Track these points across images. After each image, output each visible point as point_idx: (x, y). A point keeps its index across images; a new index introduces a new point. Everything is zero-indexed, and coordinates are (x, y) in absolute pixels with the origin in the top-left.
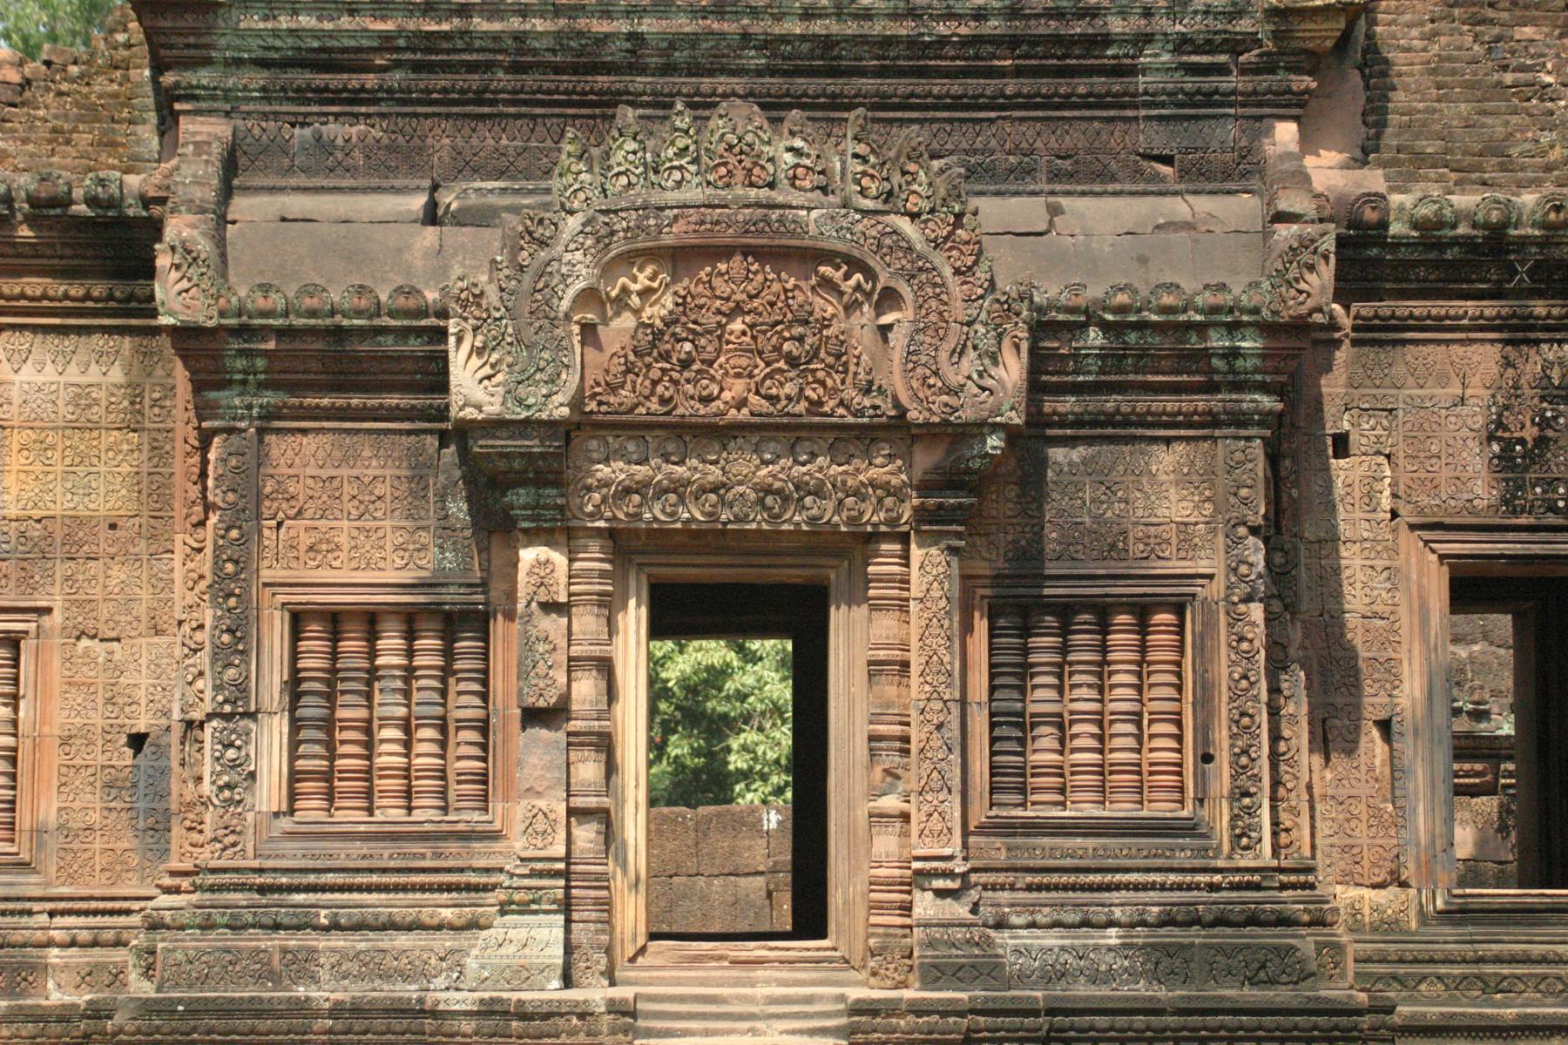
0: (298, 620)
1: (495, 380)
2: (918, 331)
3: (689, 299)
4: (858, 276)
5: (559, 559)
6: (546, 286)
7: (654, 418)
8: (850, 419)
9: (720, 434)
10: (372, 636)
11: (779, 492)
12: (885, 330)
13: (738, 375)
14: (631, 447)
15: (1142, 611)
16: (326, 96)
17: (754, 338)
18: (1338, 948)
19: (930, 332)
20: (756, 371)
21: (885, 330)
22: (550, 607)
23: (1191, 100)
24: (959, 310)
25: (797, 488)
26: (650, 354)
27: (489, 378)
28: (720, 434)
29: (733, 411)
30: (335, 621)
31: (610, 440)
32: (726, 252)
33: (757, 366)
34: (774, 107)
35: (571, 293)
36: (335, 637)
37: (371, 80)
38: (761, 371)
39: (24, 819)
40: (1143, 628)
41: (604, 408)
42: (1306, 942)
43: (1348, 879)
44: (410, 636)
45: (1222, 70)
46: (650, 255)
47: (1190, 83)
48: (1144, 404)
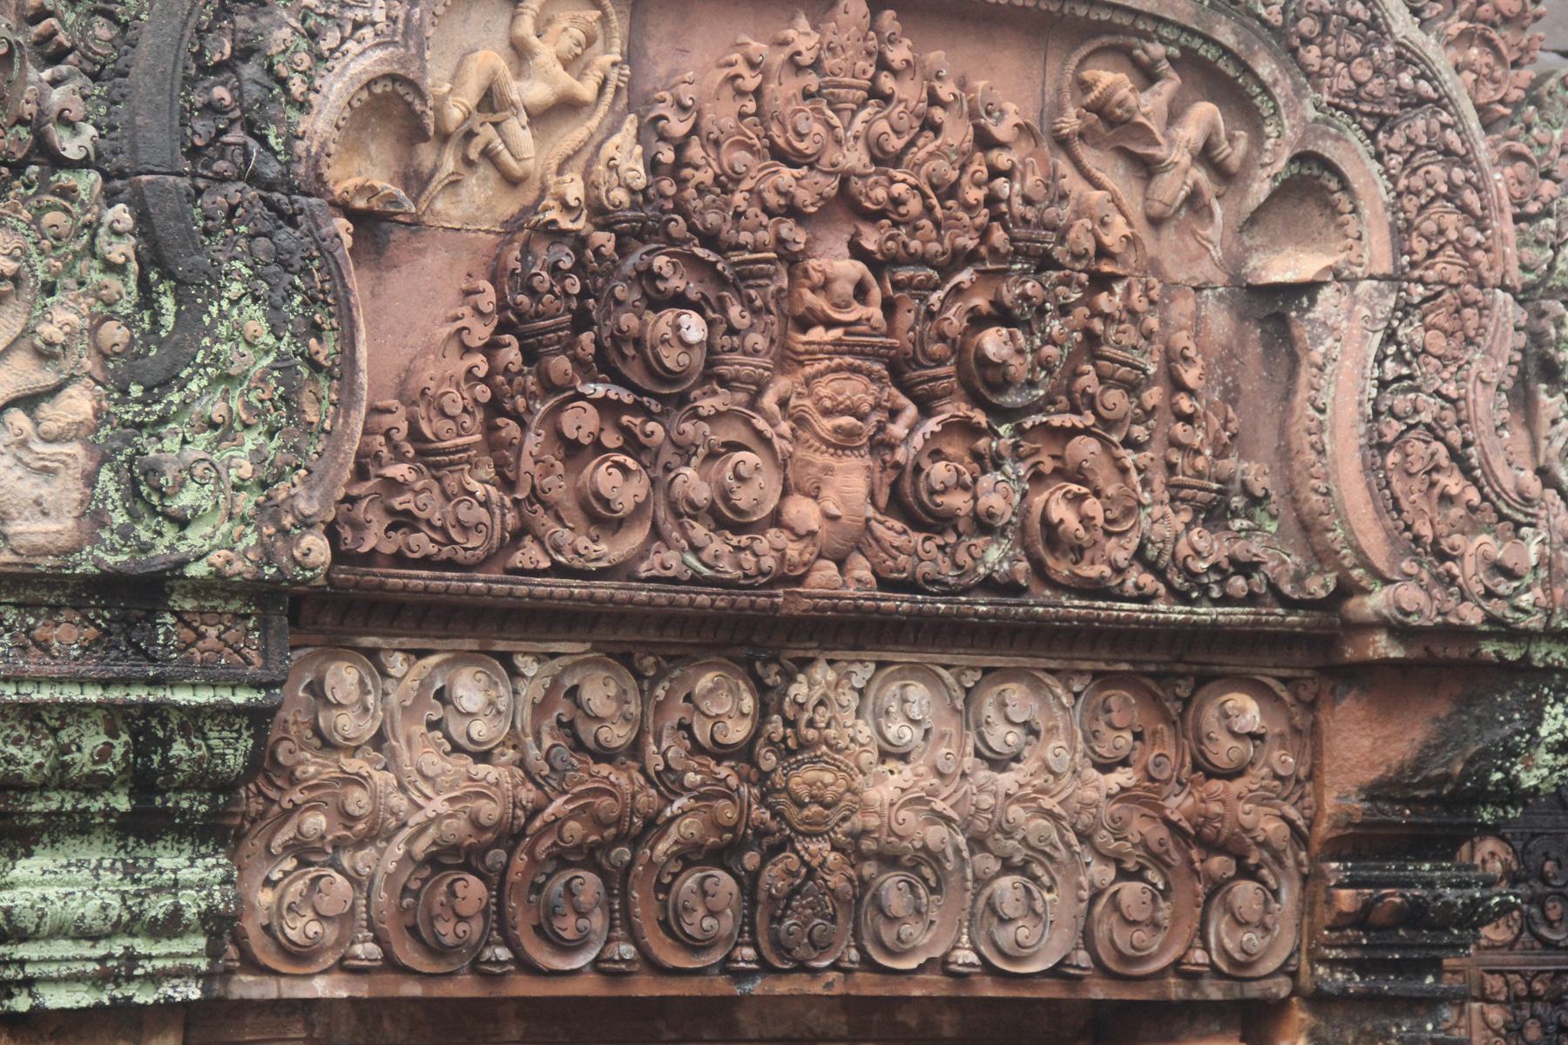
1: (58, 414)
2: (1405, 309)
3: (695, 151)
4: (1204, 114)
6: (245, 52)
7: (578, 588)
8: (1168, 611)
11: (921, 865)
12: (1274, 309)
13: (843, 443)
14: (470, 689)
17: (889, 307)
19: (1440, 318)
20: (898, 429)
21: (1274, 309)
24: (1509, 251)
25: (978, 843)
26: (569, 347)
27: (29, 402)
29: (827, 571)
31: (529, 667)
33: (894, 414)
35: (336, 90)
38: (911, 432)
41: (421, 543)
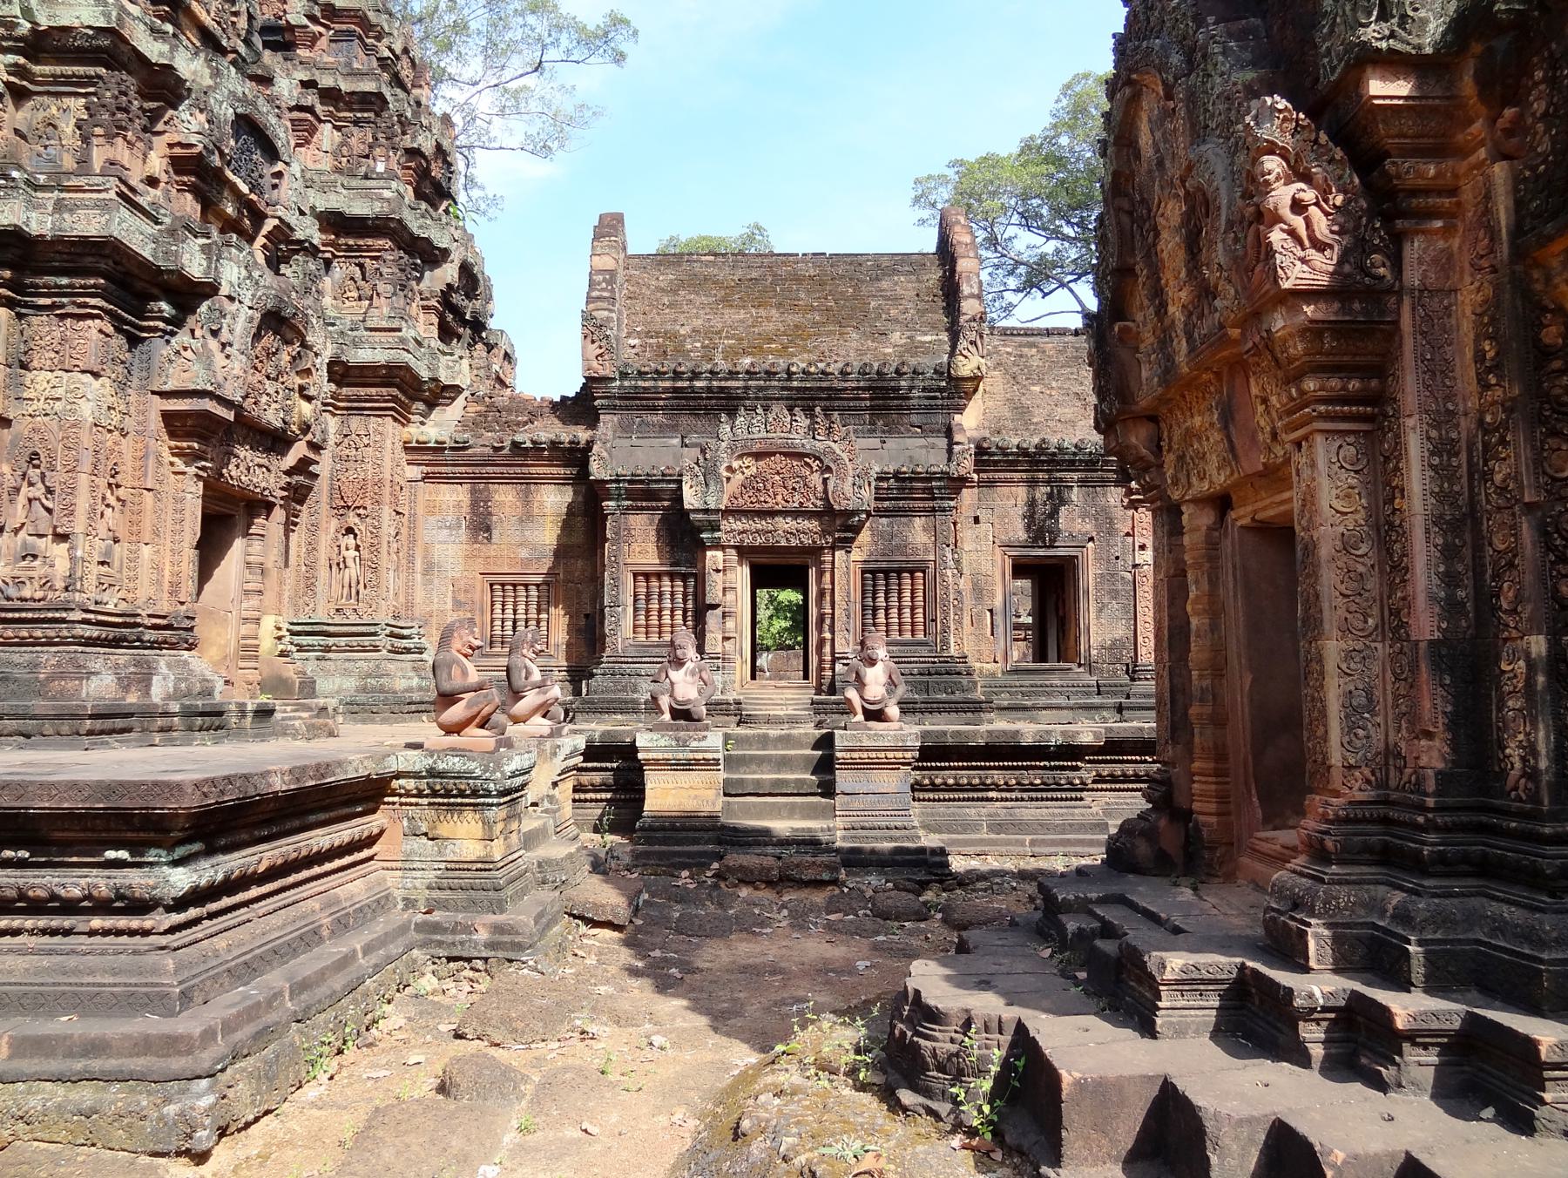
0: (635, 575)
5: (719, 554)
9: (772, 513)
10: (660, 580)
15: (912, 572)
16: (648, 408)
18: (975, 683)
22: (718, 571)
23: (926, 408)
24: (851, 473)
28: (772, 513)
30: (647, 576)
32: (774, 454)
34: (790, 409)
36: (647, 581)
37: (661, 403)
39: (552, 641)
40: (912, 578)
42: (964, 681)
43: (979, 660)
44: (672, 581)
45: (935, 398)
46: (749, 455)
47: (927, 402)
48: (912, 504)
